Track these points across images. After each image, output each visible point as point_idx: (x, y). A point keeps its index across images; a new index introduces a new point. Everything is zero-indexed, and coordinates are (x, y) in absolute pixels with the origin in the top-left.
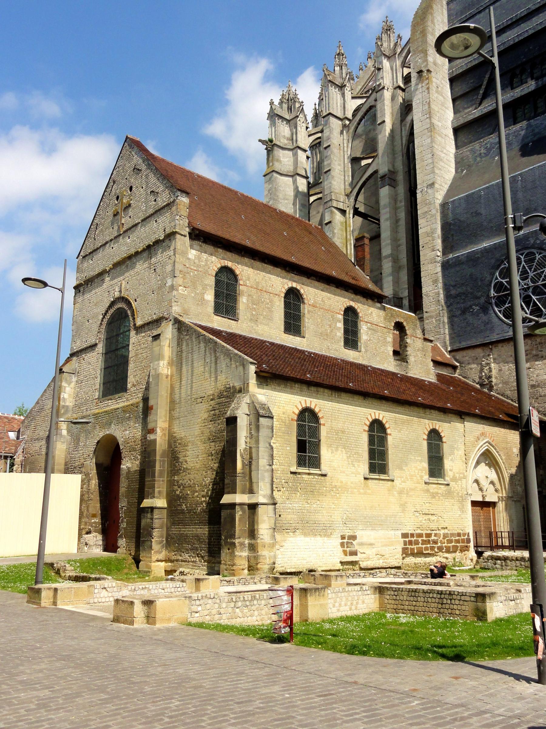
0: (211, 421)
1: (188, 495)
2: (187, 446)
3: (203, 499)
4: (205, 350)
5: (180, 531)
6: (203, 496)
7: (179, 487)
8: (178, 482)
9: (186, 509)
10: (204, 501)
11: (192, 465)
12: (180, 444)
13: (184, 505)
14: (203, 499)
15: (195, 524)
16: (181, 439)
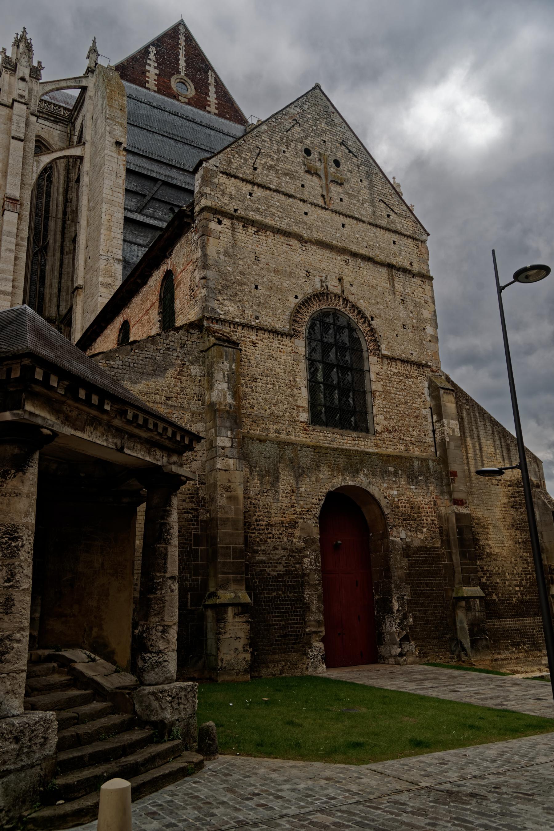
0: (512, 507)
1: (498, 583)
2: (487, 528)
3: (517, 589)
4: (493, 431)
5: (494, 625)
6: (516, 586)
7: (485, 574)
8: (482, 568)
9: (497, 600)
10: (519, 591)
11: (497, 551)
12: (477, 524)
13: (494, 595)
14: (517, 589)
15: (513, 616)
16: (478, 518)
